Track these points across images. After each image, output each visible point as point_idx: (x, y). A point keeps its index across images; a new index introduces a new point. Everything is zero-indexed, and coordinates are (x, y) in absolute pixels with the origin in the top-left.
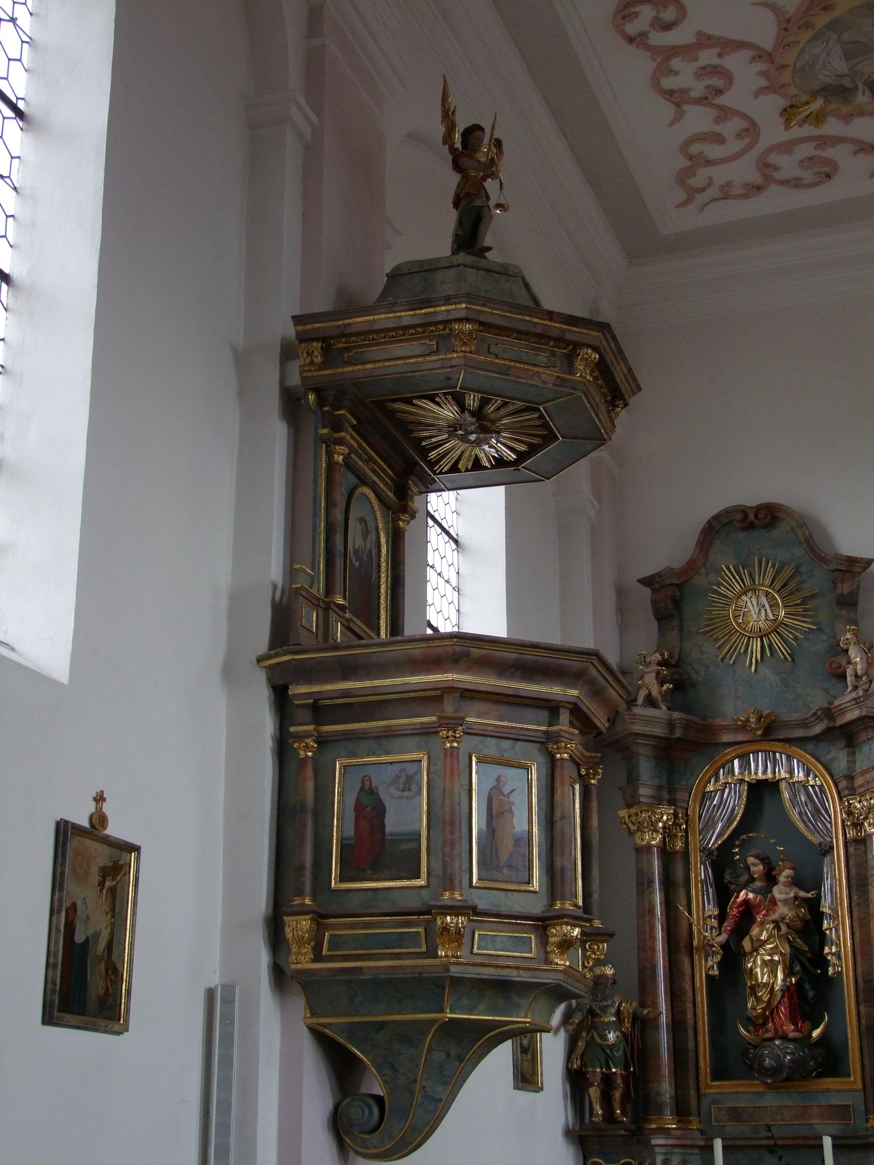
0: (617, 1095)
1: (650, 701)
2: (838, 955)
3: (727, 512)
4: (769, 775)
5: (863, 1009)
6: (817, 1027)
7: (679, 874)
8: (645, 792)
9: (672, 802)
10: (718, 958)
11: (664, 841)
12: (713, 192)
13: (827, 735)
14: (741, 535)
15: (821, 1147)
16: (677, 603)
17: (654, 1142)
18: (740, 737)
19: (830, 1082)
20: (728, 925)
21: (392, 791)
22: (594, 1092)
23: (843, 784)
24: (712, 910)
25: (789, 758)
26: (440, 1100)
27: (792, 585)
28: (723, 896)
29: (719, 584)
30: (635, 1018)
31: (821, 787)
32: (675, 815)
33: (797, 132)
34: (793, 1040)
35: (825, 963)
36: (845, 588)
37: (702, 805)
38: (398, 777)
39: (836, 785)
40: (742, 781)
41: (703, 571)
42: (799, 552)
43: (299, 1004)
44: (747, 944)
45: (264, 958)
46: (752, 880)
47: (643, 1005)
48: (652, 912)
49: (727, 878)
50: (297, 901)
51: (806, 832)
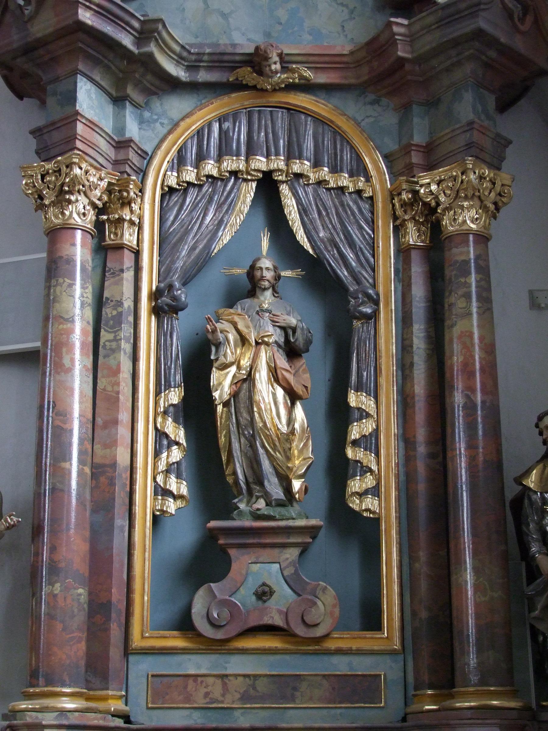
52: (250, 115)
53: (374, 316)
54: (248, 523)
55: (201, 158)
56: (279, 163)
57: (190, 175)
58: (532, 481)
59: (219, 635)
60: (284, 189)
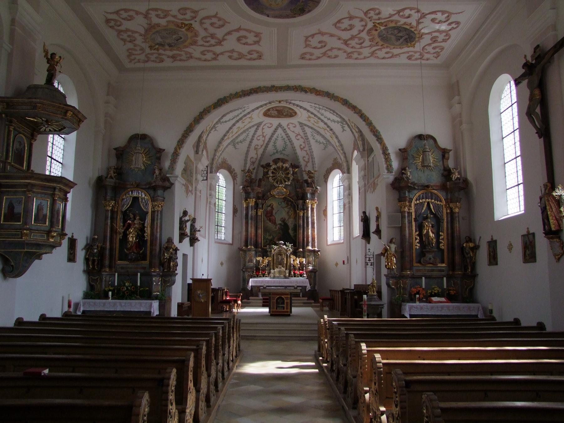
0: (96, 263)
1: (111, 177)
2: (147, 235)
6: (141, 250)
8: (108, 198)
9: (115, 200)
10: (122, 235)
11: (112, 208)
12: (135, 61)
13: (149, 188)
15: (138, 275)
17: (103, 273)
18: (132, 187)
19: (143, 262)
20: (125, 228)
22: (90, 263)
24: (122, 224)
25: (142, 192)
26: (26, 266)
27: (148, 153)
28: (125, 221)
29: (131, 151)
30: (101, 247)
31: (148, 200)
32: (115, 203)
33: (153, 51)
34: (136, 253)
35: (144, 237)
36: (158, 155)
37: (122, 201)
39: (151, 199)
40: (131, 197)
46: (131, 218)
48: (107, 224)
51: (144, 209)
52: (426, 194)
53: (443, 222)
54: (428, 250)
55: (419, 200)
57: (418, 202)
58: (464, 245)
59: (424, 264)
60: (430, 204)
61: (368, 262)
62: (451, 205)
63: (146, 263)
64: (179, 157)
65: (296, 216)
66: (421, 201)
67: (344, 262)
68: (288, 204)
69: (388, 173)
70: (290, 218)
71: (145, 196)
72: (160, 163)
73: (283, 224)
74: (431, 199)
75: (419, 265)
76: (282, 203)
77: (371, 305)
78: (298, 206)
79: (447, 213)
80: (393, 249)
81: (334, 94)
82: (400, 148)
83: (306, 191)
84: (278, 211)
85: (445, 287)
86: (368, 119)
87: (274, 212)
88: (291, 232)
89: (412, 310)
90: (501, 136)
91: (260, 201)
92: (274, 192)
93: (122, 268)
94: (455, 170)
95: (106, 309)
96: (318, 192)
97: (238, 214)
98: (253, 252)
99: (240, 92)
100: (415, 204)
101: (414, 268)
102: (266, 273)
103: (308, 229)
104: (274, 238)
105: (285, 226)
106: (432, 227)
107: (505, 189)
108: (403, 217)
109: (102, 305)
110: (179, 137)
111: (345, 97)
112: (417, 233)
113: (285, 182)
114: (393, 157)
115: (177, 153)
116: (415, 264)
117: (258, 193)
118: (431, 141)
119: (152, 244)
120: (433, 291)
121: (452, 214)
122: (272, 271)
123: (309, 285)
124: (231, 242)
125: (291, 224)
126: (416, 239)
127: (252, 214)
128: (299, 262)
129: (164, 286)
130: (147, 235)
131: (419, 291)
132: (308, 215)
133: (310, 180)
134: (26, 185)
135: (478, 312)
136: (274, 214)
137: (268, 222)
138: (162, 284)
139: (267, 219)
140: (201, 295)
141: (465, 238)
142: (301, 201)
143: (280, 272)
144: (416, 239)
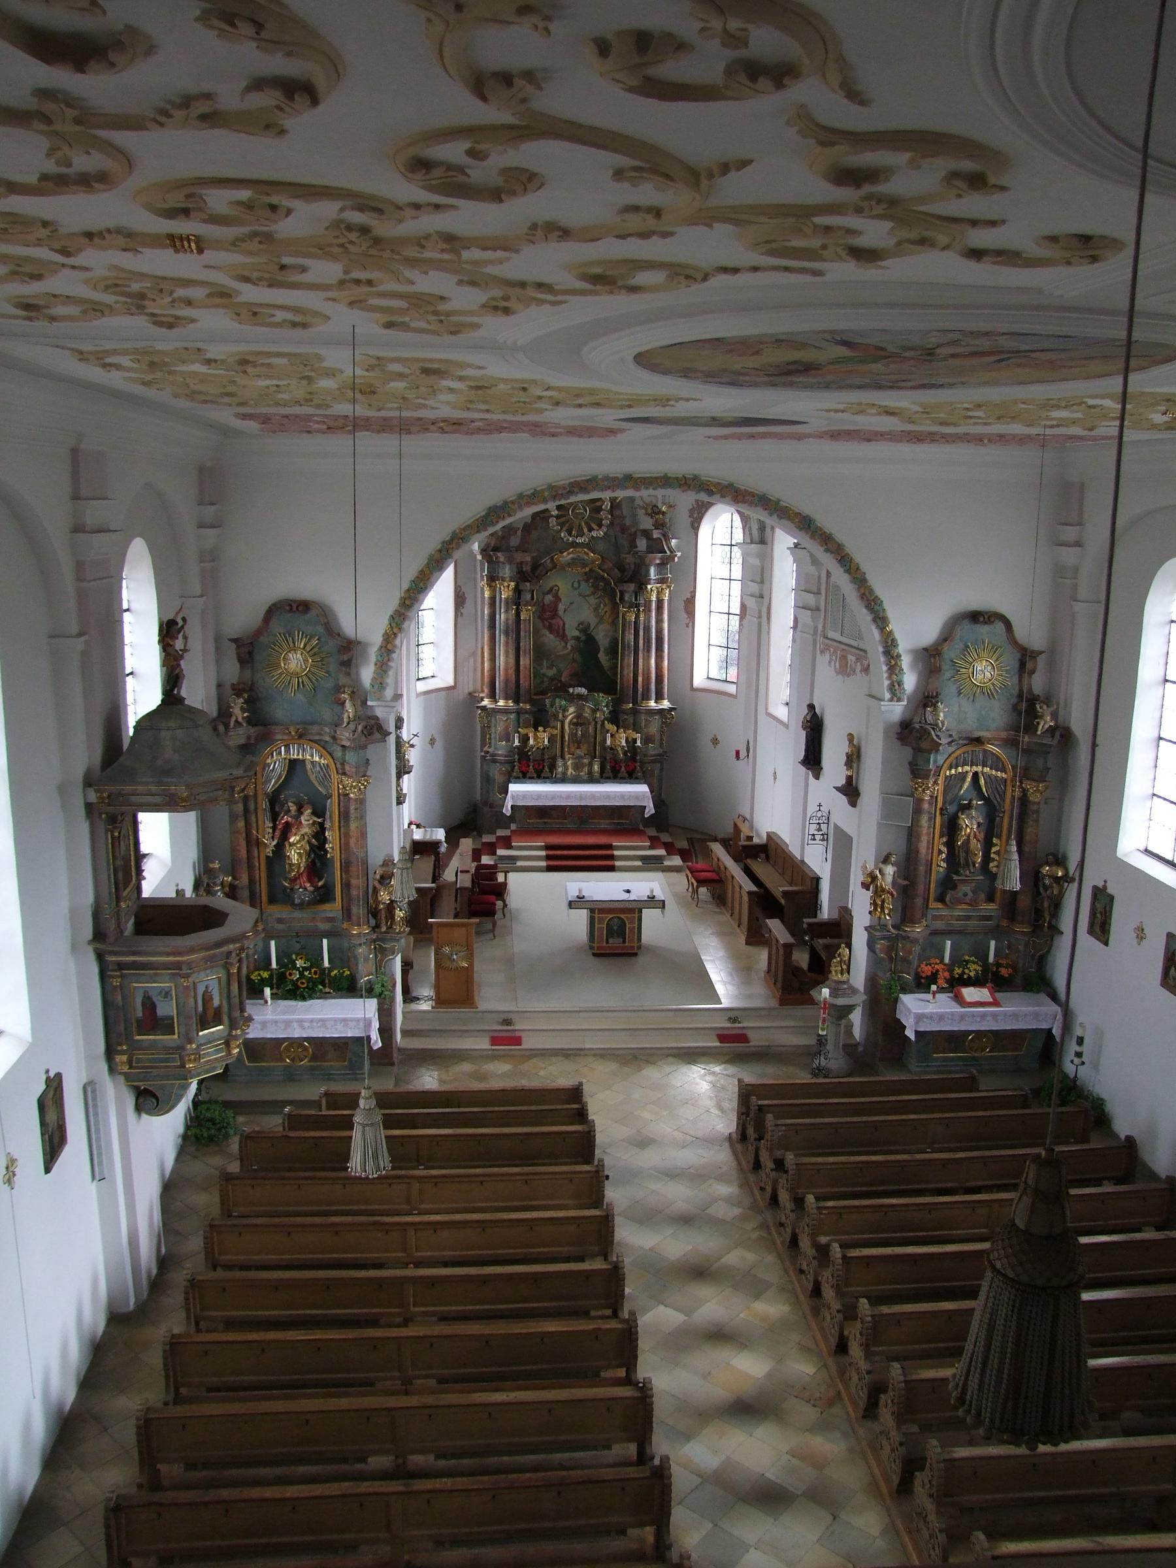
3: (280, 601)
4: (300, 757)
5: (344, 876)
6: (319, 881)
7: (252, 806)
14: (289, 615)
16: (250, 653)
18: (285, 737)
19: (327, 906)
20: (278, 833)
21: (159, 998)
23: (339, 766)
28: (275, 817)
35: (326, 852)
36: (345, 658)
37: (264, 769)
38: (161, 992)
41: (265, 634)
42: (321, 629)
43: (121, 1079)
44: (287, 844)
45: (105, 1067)
47: (234, 878)
49: (277, 809)
50: (119, 1048)
55: (956, 768)
56: (979, 769)
57: (953, 771)
60: (980, 775)
61: (816, 832)
62: (1029, 785)
63: (334, 908)
64: (394, 656)
65: (618, 617)
66: (960, 769)
67: (738, 753)
68: (596, 588)
69: (891, 700)
70: (599, 622)
71: (321, 757)
72: (349, 674)
73: (583, 638)
74: (983, 766)
75: (940, 905)
76: (583, 583)
77: (834, 1006)
78: (622, 593)
79: (1013, 797)
80: (889, 879)
81: (779, 500)
82: (924, 646)
83: (647, 562)
84: (571, 603)
85: (991, 959)
86: (858, 569)
87: (561, 607)
88: (603, 657)
89: (921, 1024)
90: (1162, 673)
91: (528, 584)
92: (567, 557)
93: (280, 921)
94: (1045, 707)
95: (269, 1036)
96: (676, 559)
97: (468, 608)
98: (512, 716)
99: (543, 491)
100: (946, 777)
101: (930, 913)
102: (546, 769)
103: (649, 658)
104: (560, 672)
105: (588, 643)
106: (979, 825)
107: (1151, 792)
108: (918, 811)
109: (259, 1027)
110: (393, 605)
111: (806, 510)
112: (945, 840)
113: (591, 529)
114: (906, 662)
115: (389, 647)
116: (933, 904)
117: (522, 563)
118: (999, 627)
119: (346, 866)
120: (966, 971)
121: (1024, 801)
122: (560, 763)
123: (652, 805)
124: (451, 682)
125: (602, 636)
126: (940, 852)
127: (507, 619)
128: (627, 741)
129: (381, 960)
130: (332, 848)
131: (937, 971)
132: (649, 622)
133: (656, 534)
134: (178, 966)
135: (1053, 1023)
136: (561, 613)
137: (546, 632)
138: (376, 956)
139: (544, 626)
140: (455, 957)
141: (1048, 855)
142: (631, 587)
143: (577, 767)
144: (940, 852)
